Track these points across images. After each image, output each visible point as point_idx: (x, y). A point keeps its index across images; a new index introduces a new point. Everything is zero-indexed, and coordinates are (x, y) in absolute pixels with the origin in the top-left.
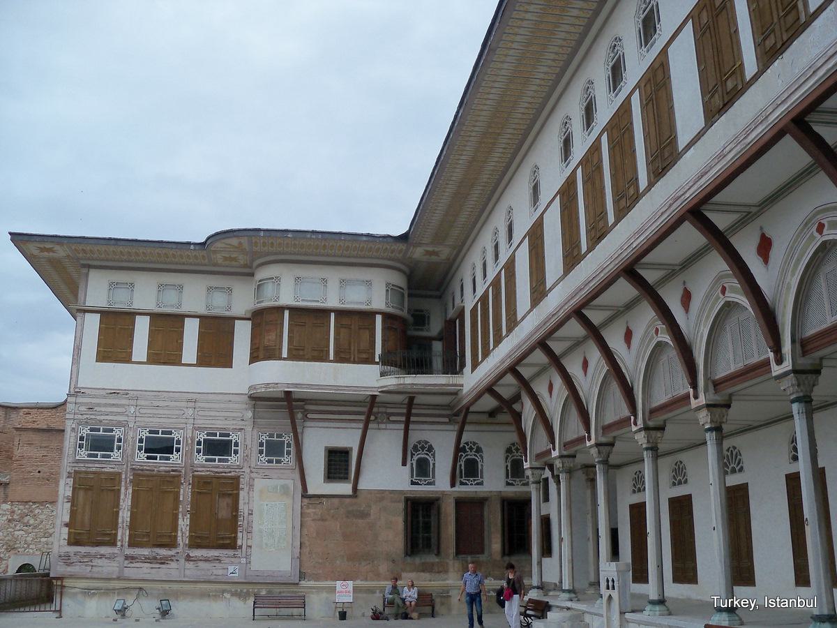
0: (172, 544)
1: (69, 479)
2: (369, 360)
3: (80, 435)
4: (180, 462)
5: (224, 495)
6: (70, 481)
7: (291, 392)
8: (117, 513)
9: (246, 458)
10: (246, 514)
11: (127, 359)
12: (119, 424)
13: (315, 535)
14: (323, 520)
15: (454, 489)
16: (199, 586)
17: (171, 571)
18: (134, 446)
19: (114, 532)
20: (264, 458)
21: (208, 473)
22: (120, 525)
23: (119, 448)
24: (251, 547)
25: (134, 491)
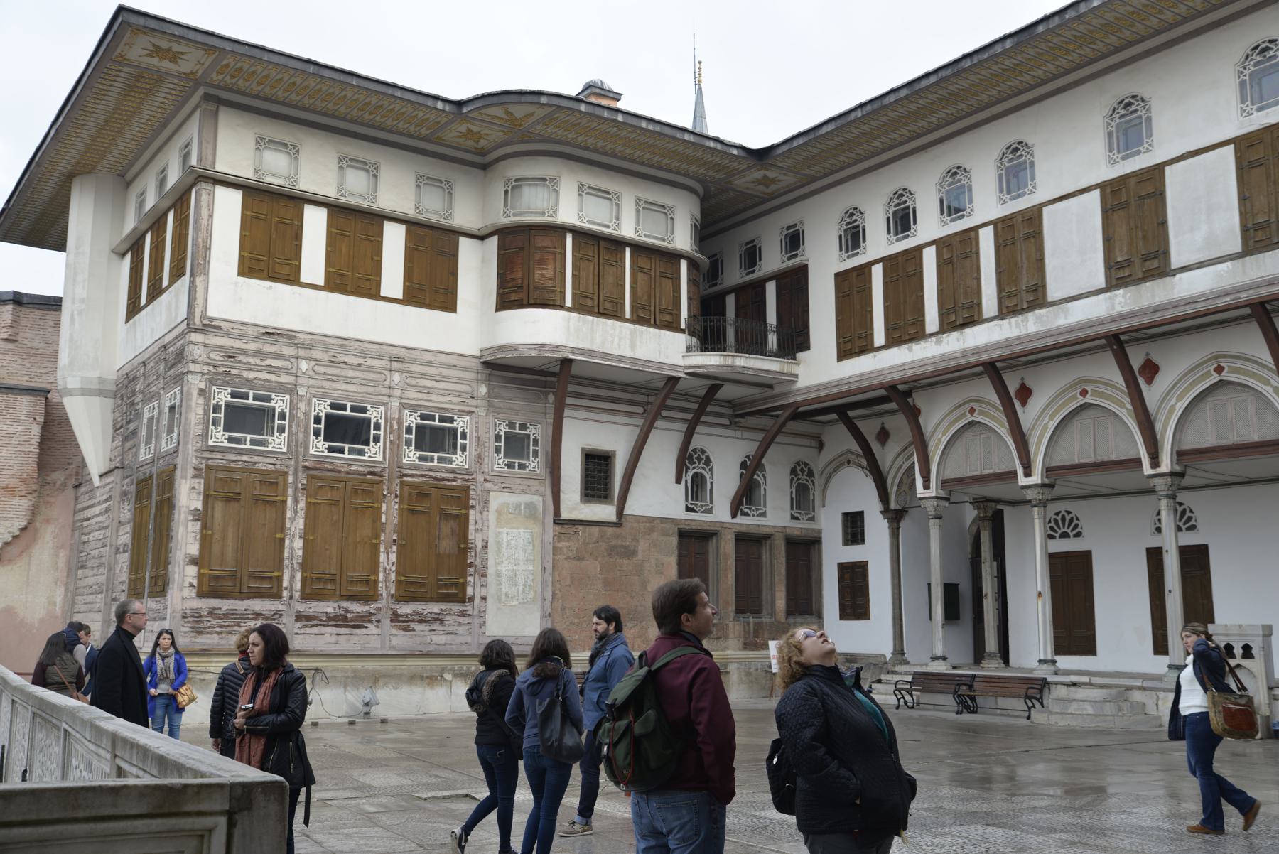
0: (369, 595)
2: (673, 326)
3: (213, 402)
4: (380, 459)
5: (446, 516)
6: (200, 484)
7: (571, 361)
8: (282, 541)
9: (479, 458)
10: (479, 544)
11: (292, 278)
12: (281, 389)
13: (568, 582)
14: (579, 558)
15: (735, 521)
16: (410, 663)
17: (372, 638)
18: (307, 428)
19: (276, 574)
20: (502, 460)
21: (421, 479)
22: (286, 562)
23: (282, 430)
24: (484, 599)
25: (308, 504)
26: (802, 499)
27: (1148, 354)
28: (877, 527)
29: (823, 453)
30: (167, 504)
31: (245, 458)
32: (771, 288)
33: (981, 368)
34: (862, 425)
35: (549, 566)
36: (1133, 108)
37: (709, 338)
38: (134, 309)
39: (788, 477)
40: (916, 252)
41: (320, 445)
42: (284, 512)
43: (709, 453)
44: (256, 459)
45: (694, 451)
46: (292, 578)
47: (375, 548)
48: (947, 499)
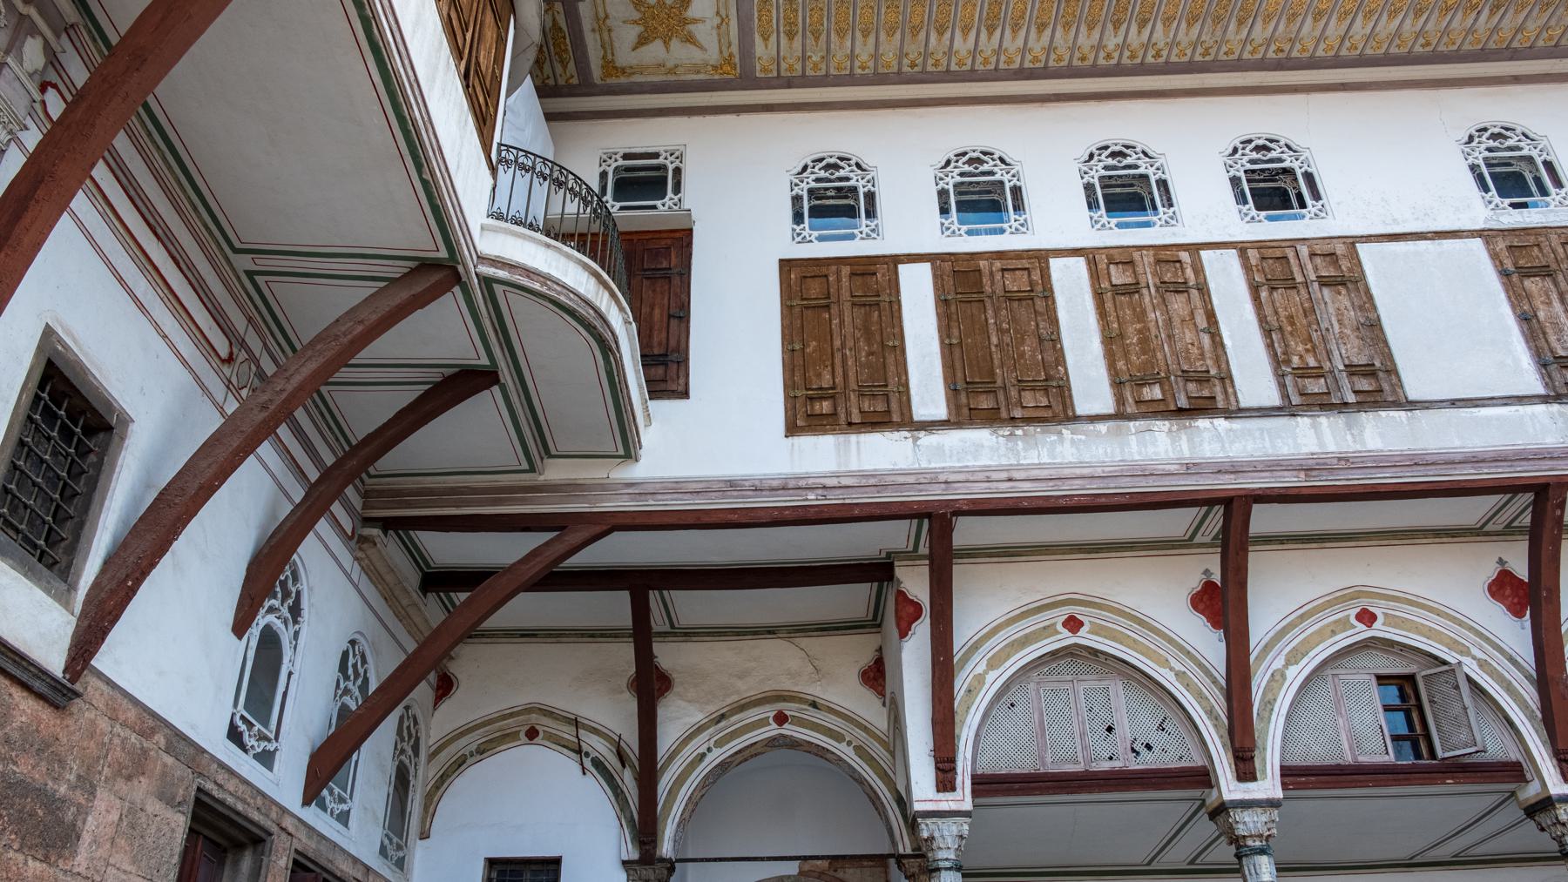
29: (447, 706)
33: (1176, 523)
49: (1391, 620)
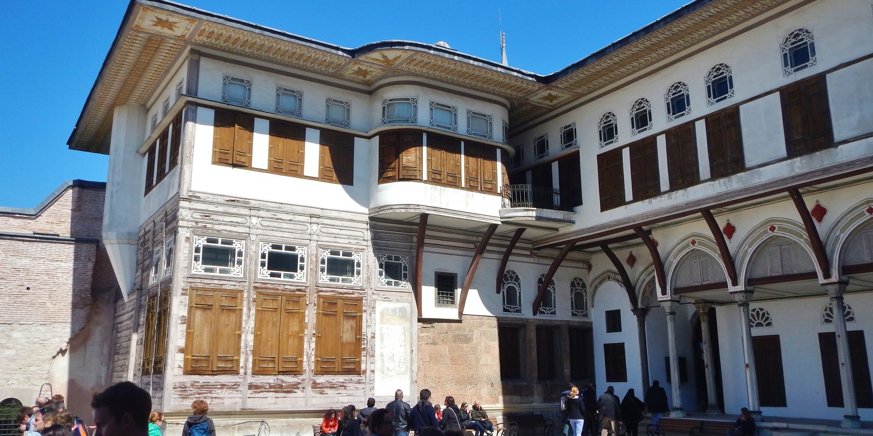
1: (184, 297)
2: (492, 191)
3: (195, 246)
5: (348, 317)
7: (427, 214)
8: (240, 336)
10: (369, 336)
12: (241, 237)
14: (434, 343)
15: (535, 317)
19: (236, 358)
21: (331, 294)
22: (242, 350)
24: (373, 371)
25: (257, 311)
26: (579, 303)
27: (817, 201)
28: (629, 321)
30: (164, 314)
31: (216, 282)
32: (555, 166)
34: (619, 254)
35: (415, 349)
36: (800, 37)
37: (517, 199)
38: (149, 187)
39: (570, 289)
40: (653, 139)
41: (265, 272)
42: (241, 317)
43: (518, 273)
44: (223, 282)
45: (508, 272)
46: (246, 360)
47: (301, 339)
48: (678, 302)
49: (781, 229)
